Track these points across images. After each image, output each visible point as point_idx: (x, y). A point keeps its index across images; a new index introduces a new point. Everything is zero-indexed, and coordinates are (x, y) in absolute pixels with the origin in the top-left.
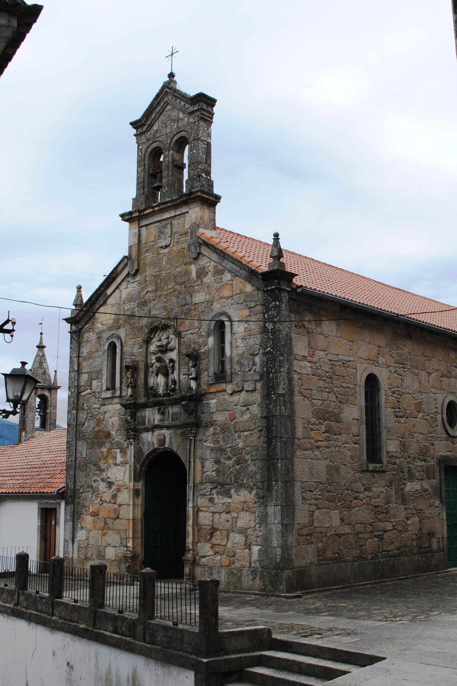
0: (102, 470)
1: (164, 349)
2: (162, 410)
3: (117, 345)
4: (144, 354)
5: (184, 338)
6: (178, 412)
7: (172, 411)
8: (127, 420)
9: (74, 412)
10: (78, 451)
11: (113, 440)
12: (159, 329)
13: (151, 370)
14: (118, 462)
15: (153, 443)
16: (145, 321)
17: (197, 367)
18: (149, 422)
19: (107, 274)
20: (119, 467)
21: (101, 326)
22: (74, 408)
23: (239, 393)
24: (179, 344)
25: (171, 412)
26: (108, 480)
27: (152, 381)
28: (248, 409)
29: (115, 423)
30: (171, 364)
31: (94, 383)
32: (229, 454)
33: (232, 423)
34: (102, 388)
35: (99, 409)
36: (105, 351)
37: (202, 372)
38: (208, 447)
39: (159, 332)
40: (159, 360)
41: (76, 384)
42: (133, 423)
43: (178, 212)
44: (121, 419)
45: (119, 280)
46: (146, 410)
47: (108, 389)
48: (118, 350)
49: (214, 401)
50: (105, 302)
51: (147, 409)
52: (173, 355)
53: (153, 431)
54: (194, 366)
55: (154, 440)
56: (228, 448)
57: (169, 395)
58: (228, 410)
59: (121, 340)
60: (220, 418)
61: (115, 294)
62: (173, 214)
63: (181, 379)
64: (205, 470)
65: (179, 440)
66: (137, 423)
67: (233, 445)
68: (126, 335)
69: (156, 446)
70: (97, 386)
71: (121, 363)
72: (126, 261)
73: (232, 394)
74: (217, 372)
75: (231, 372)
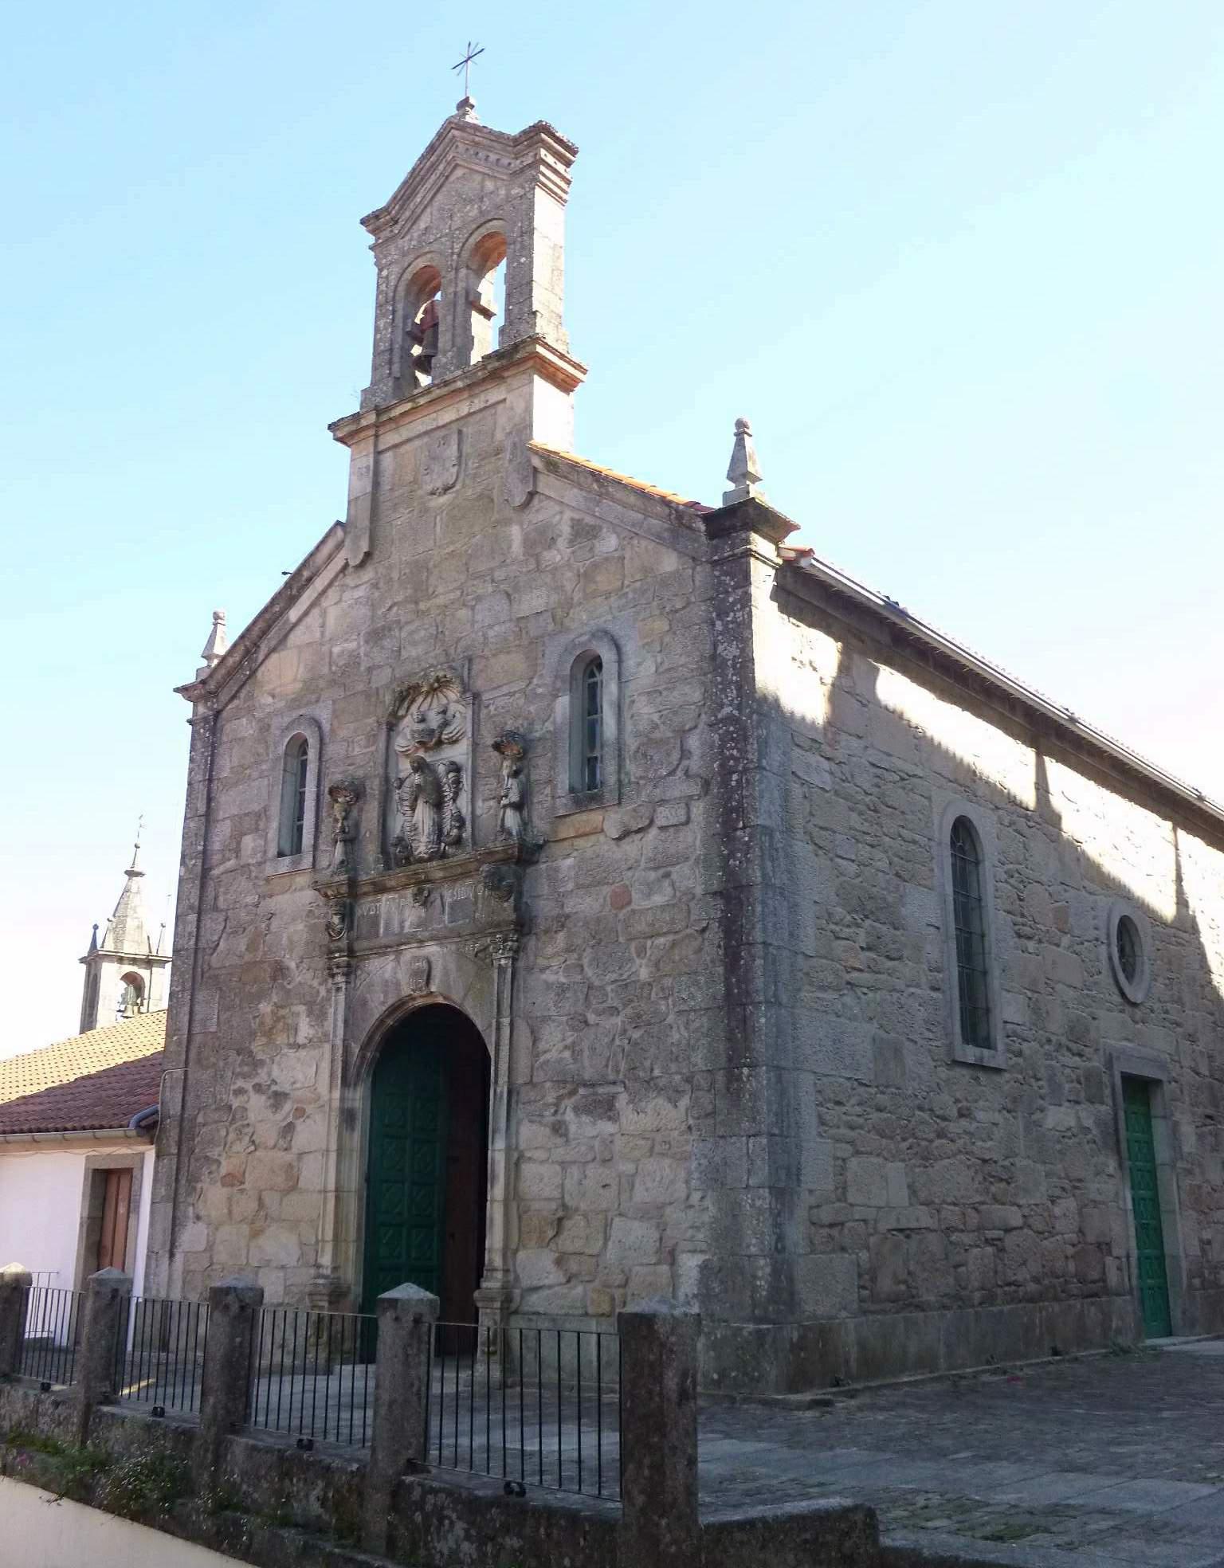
0: (257, 1064)
1: (433, 740)
2: (426, 893)
3: (310, 741)
4: (381, 759)
8: (329, 926)
9: (193, 917)
10: (197, 1017)
13: (396, 797)
14: (301, 1040)
15: (398, 984)
16: (382, 678)
17: (522, 777)
19: (292, 569)
20: (303, 1053)
21: (270, 700)
22: (191, 907)
23: (639, 836)
24: (476, 722)
25: (448, 900)
26: (274, 1088)
27: (398, 824)
28: (667, 875)
29: (295, 938)
30: (451, 775)
31: (249, 842)
32: (613, 1001)
33: (621, 916)
34: (265, 852)
36: (278, 759)
38: (548, 986)
39: (421, 699)
40: (420, 766)
41: (200, 848)
42: (344, 934)
43: (478, 404)
44: (312, 928)
45: (319, 584)
46: (379, 901)
47: (281, 854)
48: (312, 754)
49: (570, 861)
51: (384, 897)
52: (459, 753)
53: (398, 953)
54: (515, 774)
55: (400, 976)
57: (443, 856)
59: (320, 728)
60: (585, 905)
61: (308, 620)
62: (465, 409)
63: (479, 812)
64: (542, 1046)
66: (354, 933)
68: (335, 715)
69: (406, 991)
70: (254, 851)
71: (318, 786)
72: (340, 533)
73: (619, 839)
74: (578, 786)
75: (620, 781)
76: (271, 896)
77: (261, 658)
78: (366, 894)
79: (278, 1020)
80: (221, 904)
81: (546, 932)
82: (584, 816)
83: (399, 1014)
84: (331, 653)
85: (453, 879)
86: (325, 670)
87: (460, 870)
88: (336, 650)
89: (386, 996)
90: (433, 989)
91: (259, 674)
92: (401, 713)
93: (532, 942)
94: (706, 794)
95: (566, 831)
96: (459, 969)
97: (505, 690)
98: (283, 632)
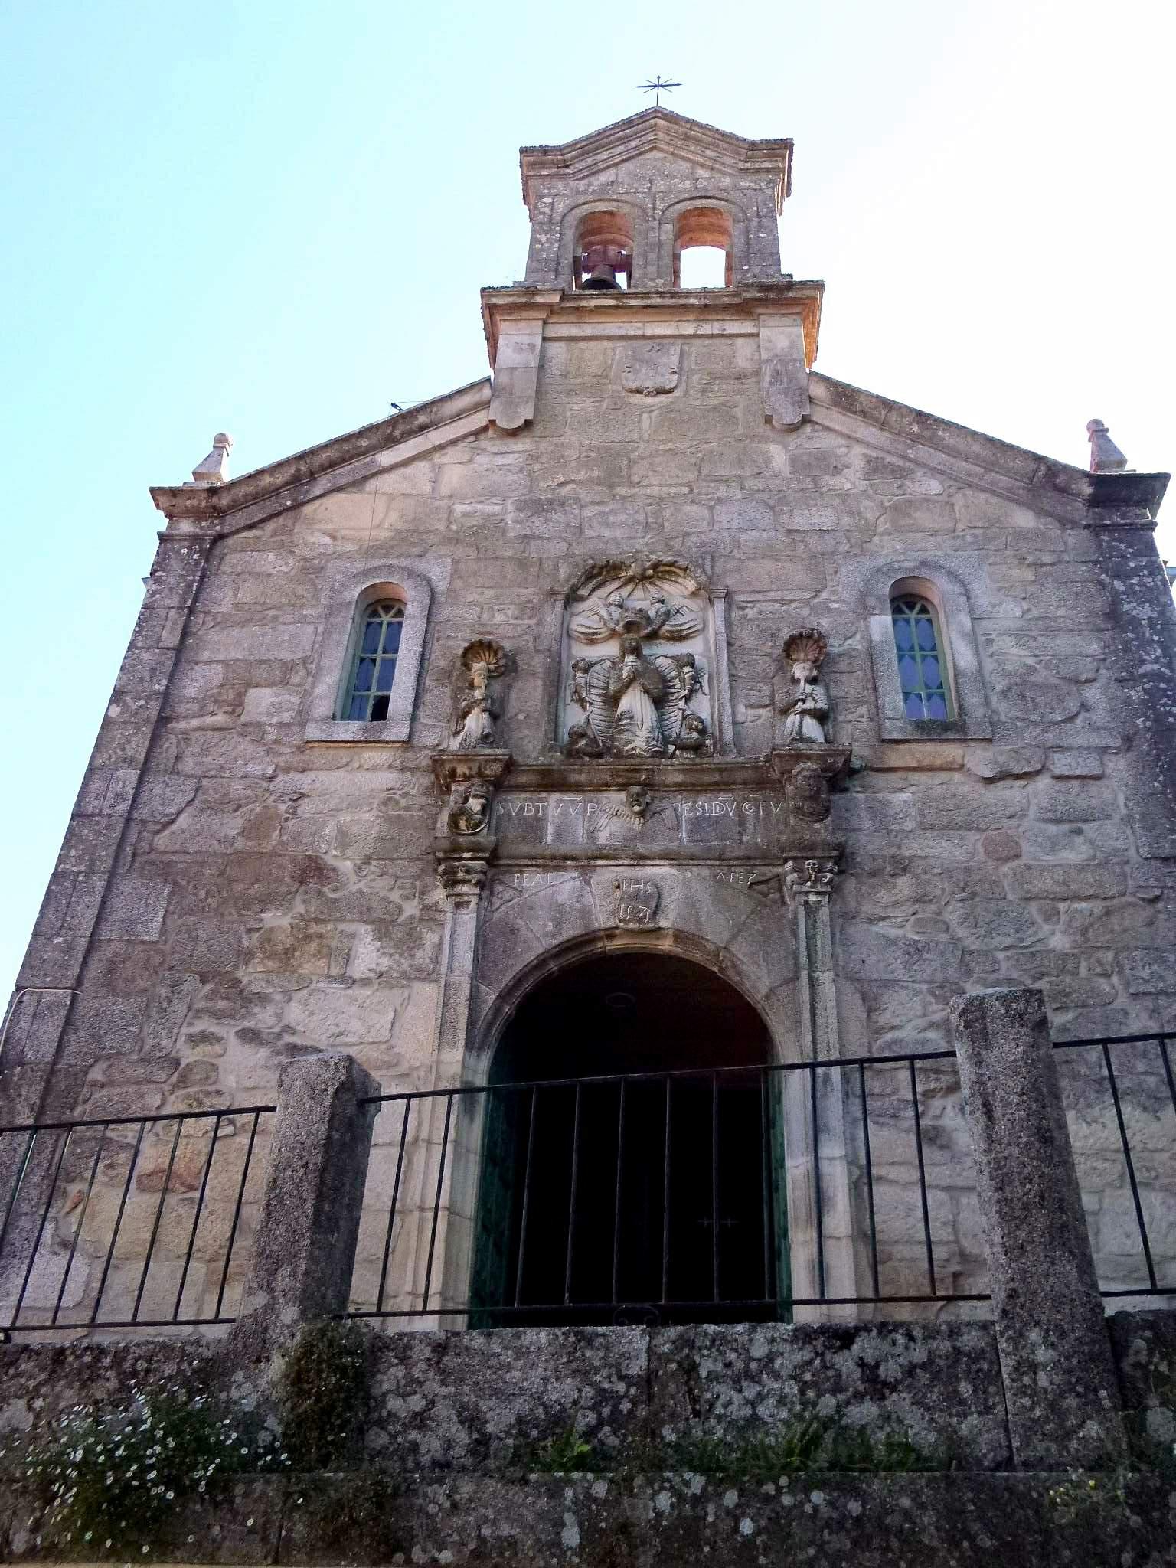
0: (246, 1000)
5: (743, 609)
6: (726, 815)
11: (335, 890)
14: (358, 970)
18: (559, 835)
19: (406, 406)
20: (358, 992)
26: (288, 1039)
28: (1079, 832)
35: (271, 779)
37: (840, 708)
38: (890, 942)
39: (616, 584)
43: (706, 329)
45: (436, 437)
50: (358, 483)
51: (555, 797)
55: (588, 900)
56: (997, 949)
58: (978, 829)
59: (429, 581)
62: (689, 329)
64: (884, 1019)
65: (744, 904)
67: (1022, 940)
69: (602, 921)
72: (487, 392)
73: (989, 781)
76: (303, 771)
77: (317, 491)
78: (521, 788)
79: (308, 938)
80: (188, 765)
81: (873, 874)
82: (929, 747)
83: (573, 957)
84: (451, 512)
85: (692, 789)
86: (441, 526)
87: (717, 777)
88: (460, 509)
89: (558, 925)
90: (663, 923)
91: (307, 509)
92: (584, 592)
93: (850, 885)
94: (1129, 749)
95: (896, 757)
96: (718, 900)
97: (773, 595)
98: (365, 473)
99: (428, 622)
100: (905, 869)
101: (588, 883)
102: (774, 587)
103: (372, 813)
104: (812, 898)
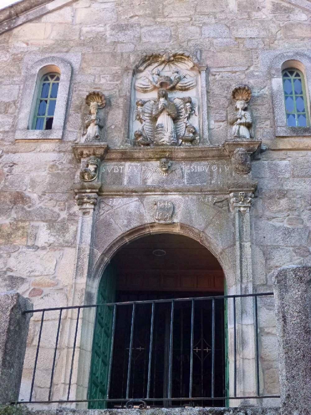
5: (215, 75)
6: (204, 172)
7: (190, 169)
11: (29, 207)
12: (157, 61)
14: (40, 242)
18: (129, 182)
20: (40, 252)
37: (258, 121)
38: (276, 229)
39: (156, 64)
50: (38, 18)
51: (128, 164)
55: (142, 210)
59: (71, 64)
69: (148, 219)
76: (15, 153)
77: (19, 22)
78: (111, 160)
79: (18, 229)
81: (271, 198)
82: (297, 140)
83: (136, 236)
84: (81, 31)
85: (190, 159)
86: (76, 38)
87: (200, 154)
88: (85, 29)
90: (175, 221)
91: (15, 31)
92: (142, 68)
93: (260, 203)
95: (282, 144)
96: (200, 211)
97: (229, 69)
98: (41, 13)
99: (71, 84)
100: (284, 196)
101: (142, 203)
102: (228, 65)
103: (45, 172)
104: (242, 209)
